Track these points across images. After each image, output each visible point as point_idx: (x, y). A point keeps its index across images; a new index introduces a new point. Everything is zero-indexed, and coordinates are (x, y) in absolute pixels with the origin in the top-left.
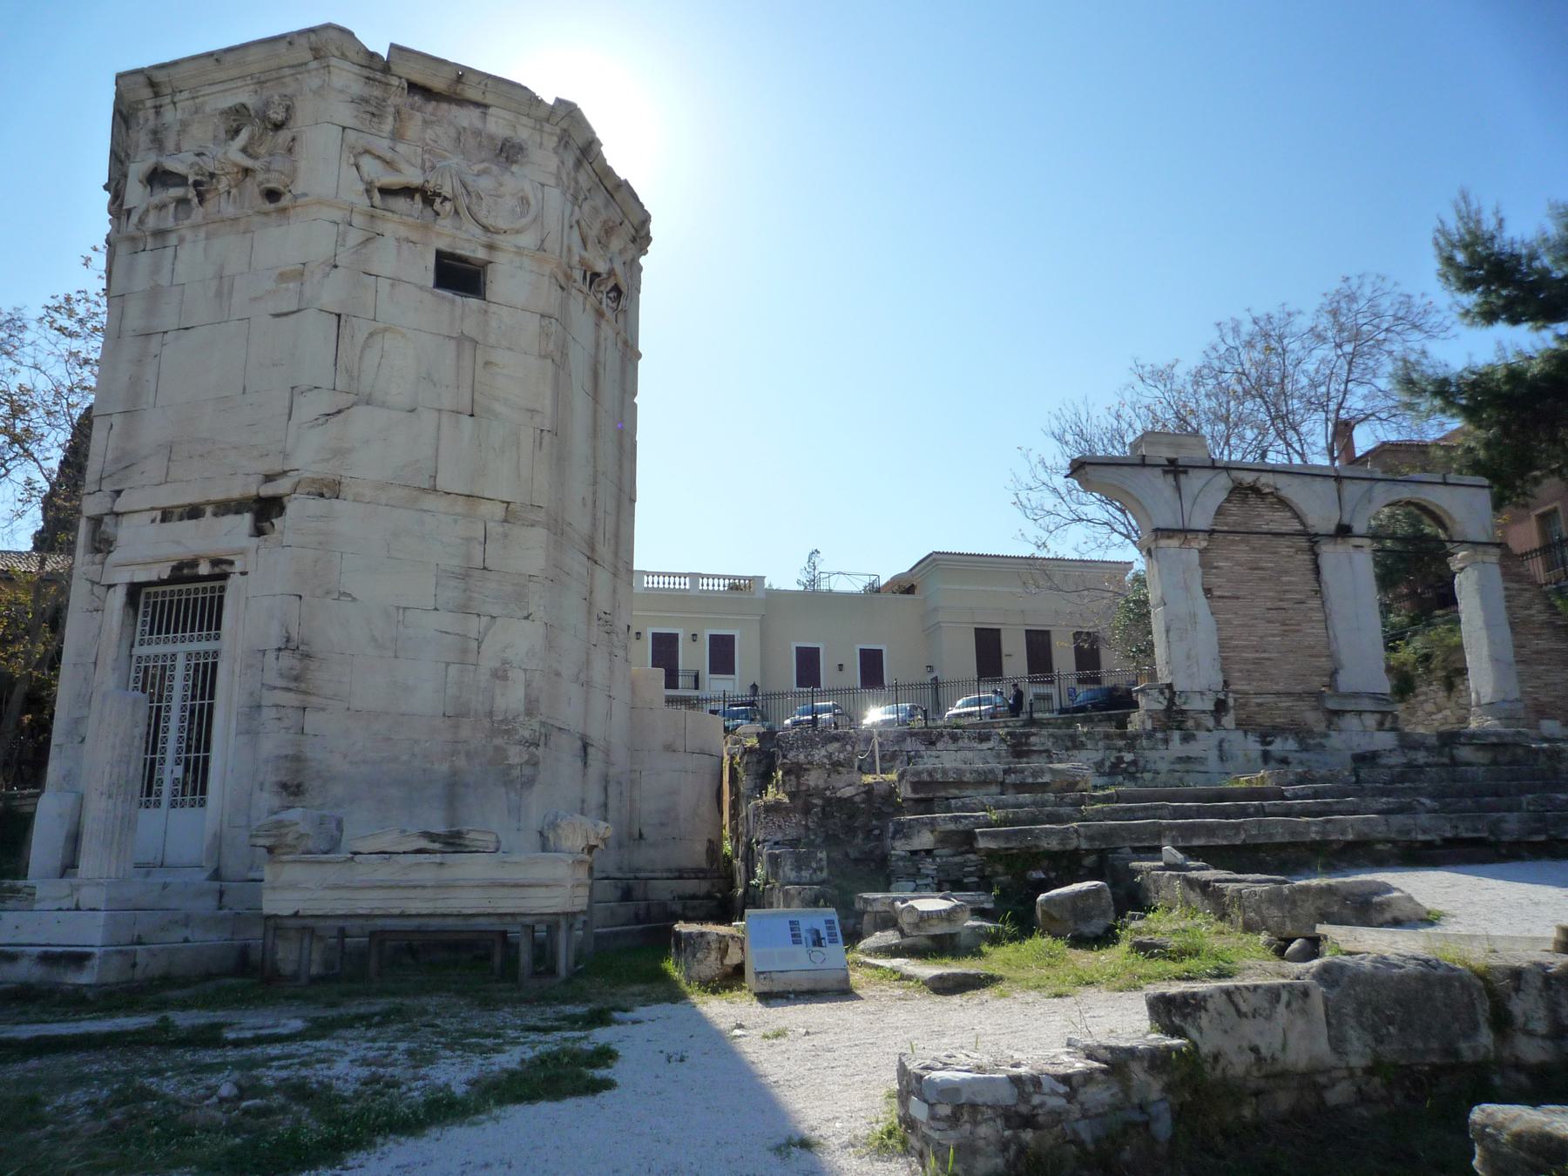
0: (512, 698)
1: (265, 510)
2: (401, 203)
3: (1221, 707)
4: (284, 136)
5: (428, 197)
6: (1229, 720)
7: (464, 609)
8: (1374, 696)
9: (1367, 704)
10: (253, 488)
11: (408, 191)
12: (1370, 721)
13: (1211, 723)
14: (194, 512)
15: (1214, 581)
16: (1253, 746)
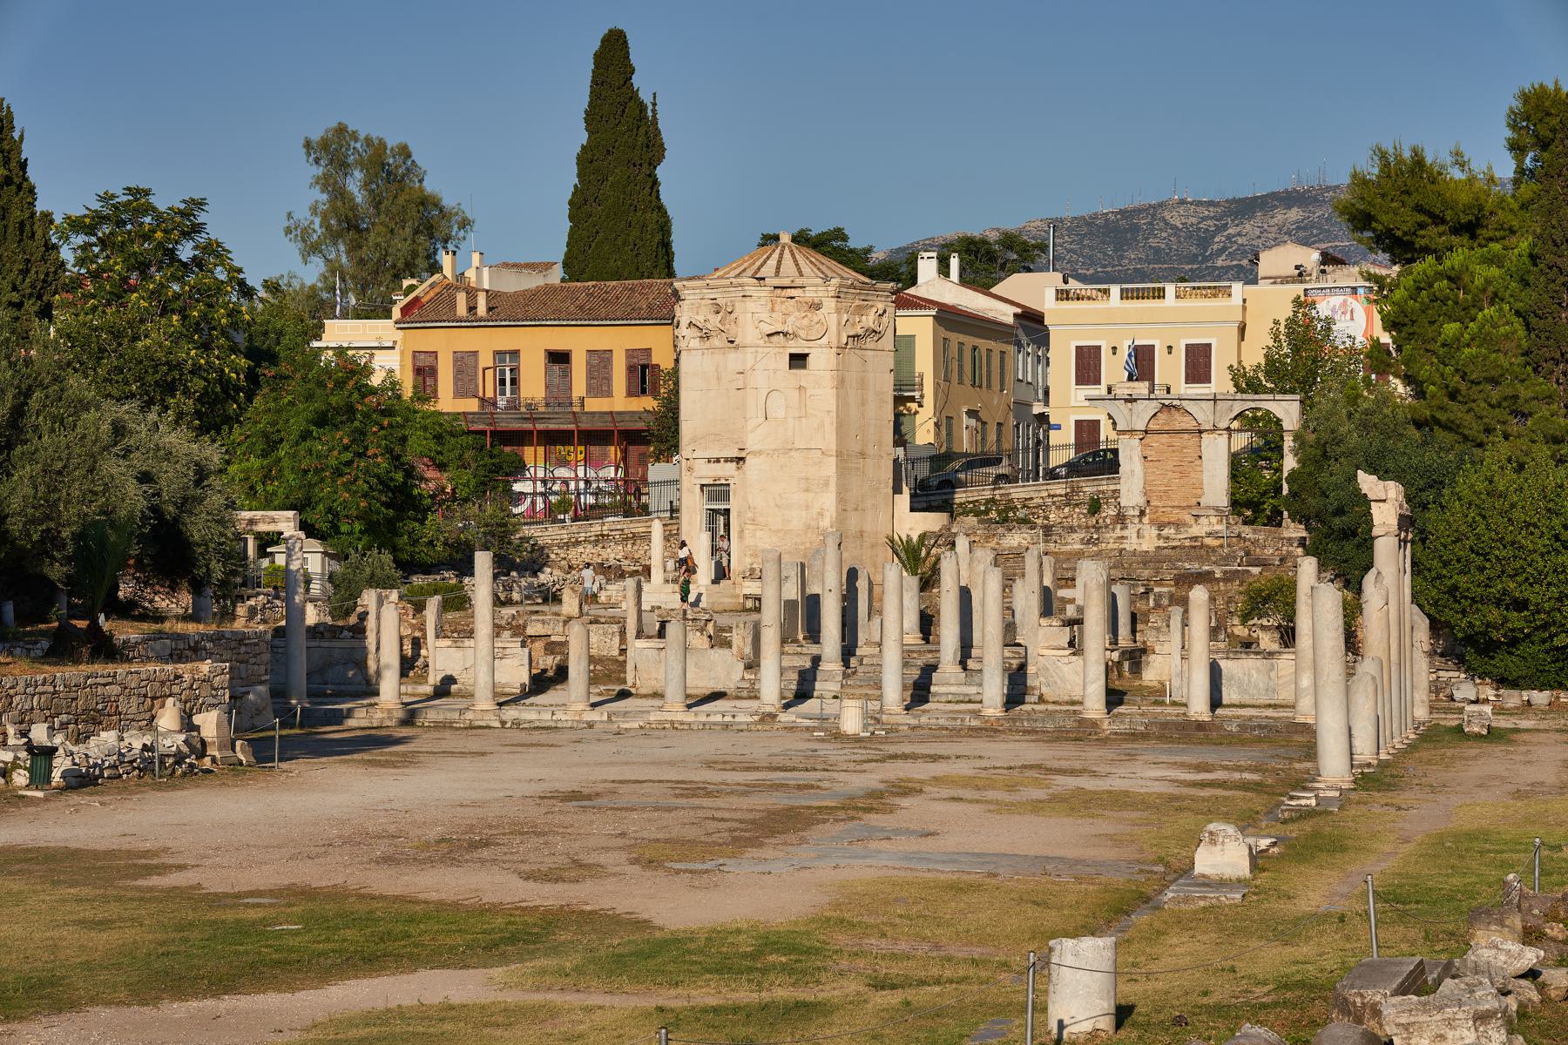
0: (826, 523)
1: (740, 460)
2: (775, 338)
3: (1142, 513)
4: (733, 316)
5: (785, 334)
6: (1146, 520)
7: (807, 490)
8: (1217, 509)
9: (1212, 512)
10: (736, 454)
11: (778, 333)
12: (1214, 520)
13: (1136, 520)
14: (718, 461)
15: (1148, 453)
16: (1155, 532)
